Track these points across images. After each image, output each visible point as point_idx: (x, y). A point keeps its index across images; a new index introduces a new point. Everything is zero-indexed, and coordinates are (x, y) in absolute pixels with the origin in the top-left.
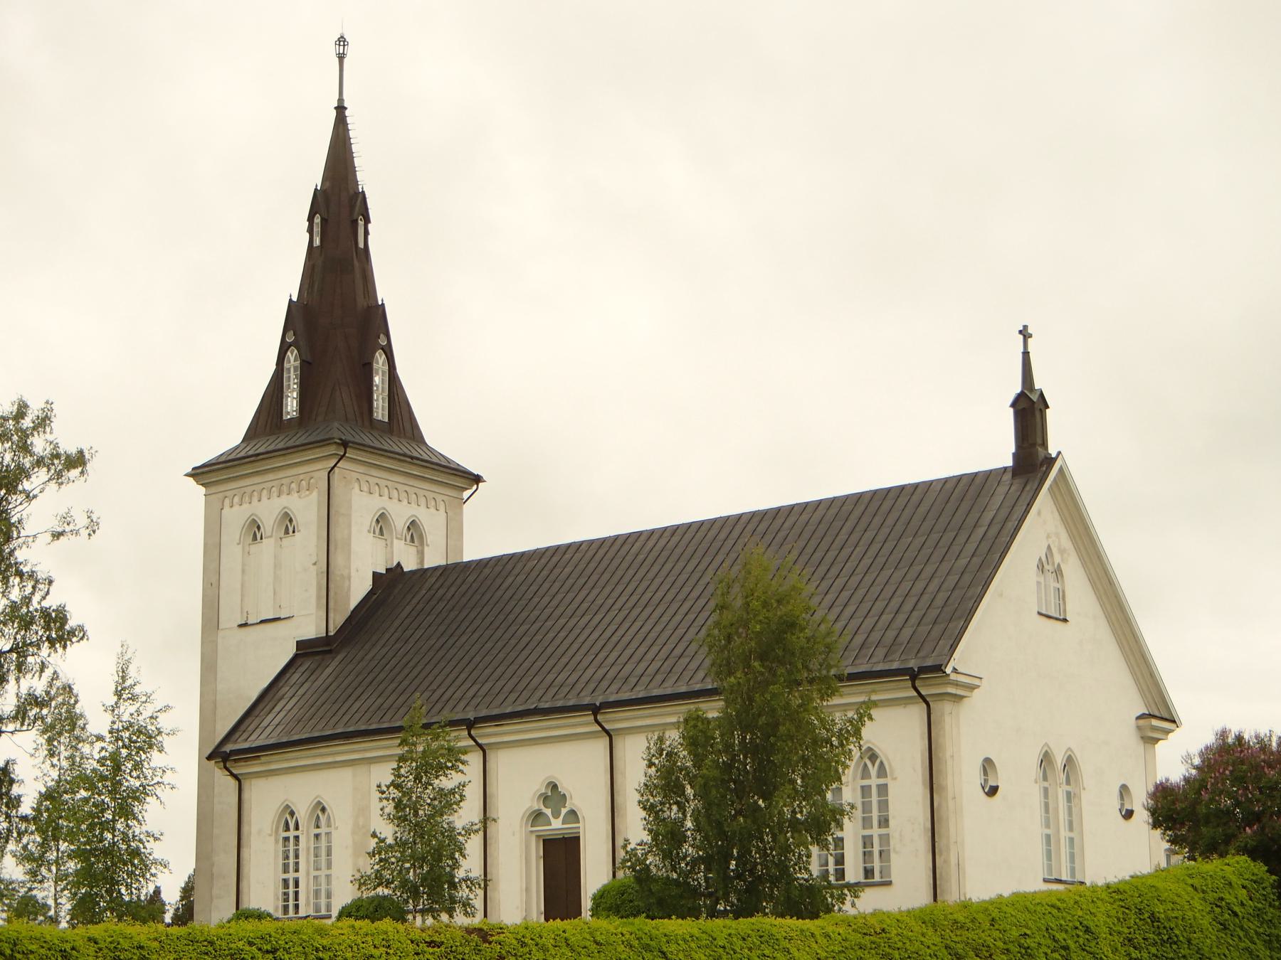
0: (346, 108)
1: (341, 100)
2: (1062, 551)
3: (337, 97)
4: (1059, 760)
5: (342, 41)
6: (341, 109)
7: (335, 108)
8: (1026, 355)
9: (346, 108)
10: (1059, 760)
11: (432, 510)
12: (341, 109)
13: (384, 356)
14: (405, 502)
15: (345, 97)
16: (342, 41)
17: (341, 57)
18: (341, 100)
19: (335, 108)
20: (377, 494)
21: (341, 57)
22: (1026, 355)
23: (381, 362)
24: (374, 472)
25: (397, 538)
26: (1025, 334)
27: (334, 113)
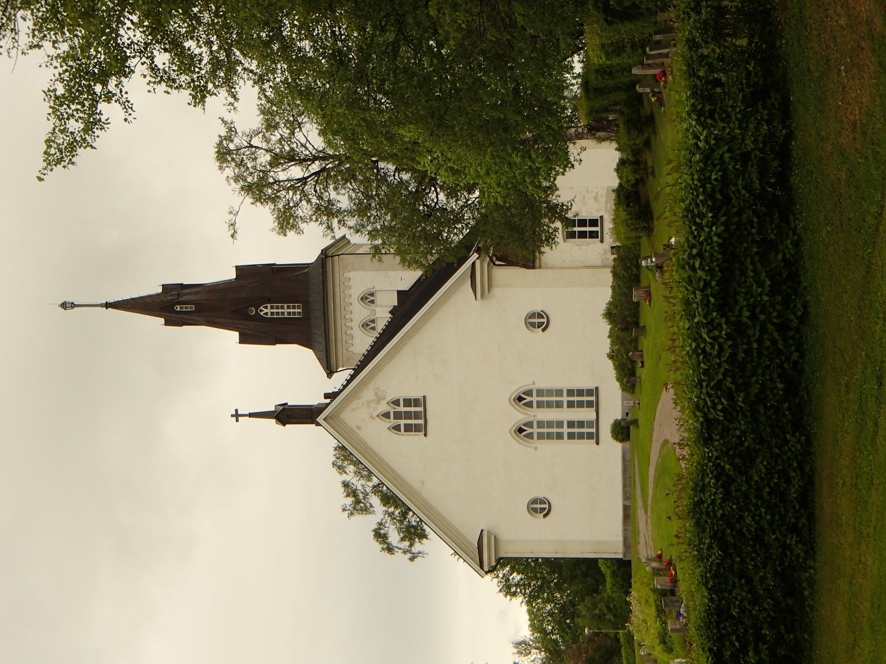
0: (106, 302)
1: (101, 305)
2: (379, 400)
3: (99, 308)
4: (520, 416)
5: (64, 306)
6: (108, 305)
7: (107, 308)
8: (251, 415)
9: (106, 302)
10: (520, 416)
11: (351, 283)
12: (108, 305)
13: (261, 308)
14: (351, 307)
15: (99, 302)
16: (64, 306)
17: (73, 306)
18: (101, 305)
19: (107, 308)
20: (352, 332)
21: (73, 306)
22: (251, 415)
23: (266, 311)
24: (339, 336)
25: (375, 315)
26: (237, 416)
27: (110, 309)
